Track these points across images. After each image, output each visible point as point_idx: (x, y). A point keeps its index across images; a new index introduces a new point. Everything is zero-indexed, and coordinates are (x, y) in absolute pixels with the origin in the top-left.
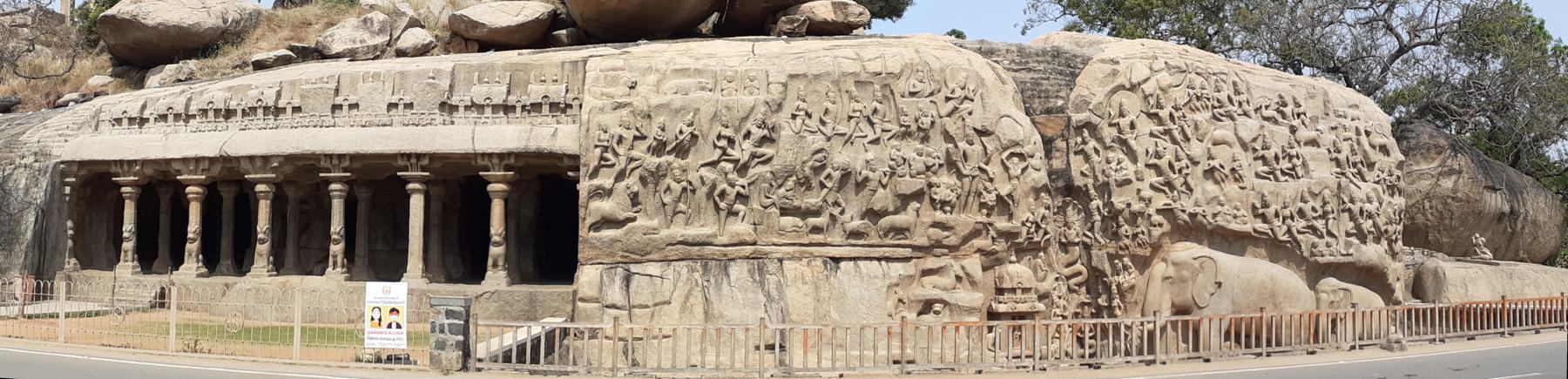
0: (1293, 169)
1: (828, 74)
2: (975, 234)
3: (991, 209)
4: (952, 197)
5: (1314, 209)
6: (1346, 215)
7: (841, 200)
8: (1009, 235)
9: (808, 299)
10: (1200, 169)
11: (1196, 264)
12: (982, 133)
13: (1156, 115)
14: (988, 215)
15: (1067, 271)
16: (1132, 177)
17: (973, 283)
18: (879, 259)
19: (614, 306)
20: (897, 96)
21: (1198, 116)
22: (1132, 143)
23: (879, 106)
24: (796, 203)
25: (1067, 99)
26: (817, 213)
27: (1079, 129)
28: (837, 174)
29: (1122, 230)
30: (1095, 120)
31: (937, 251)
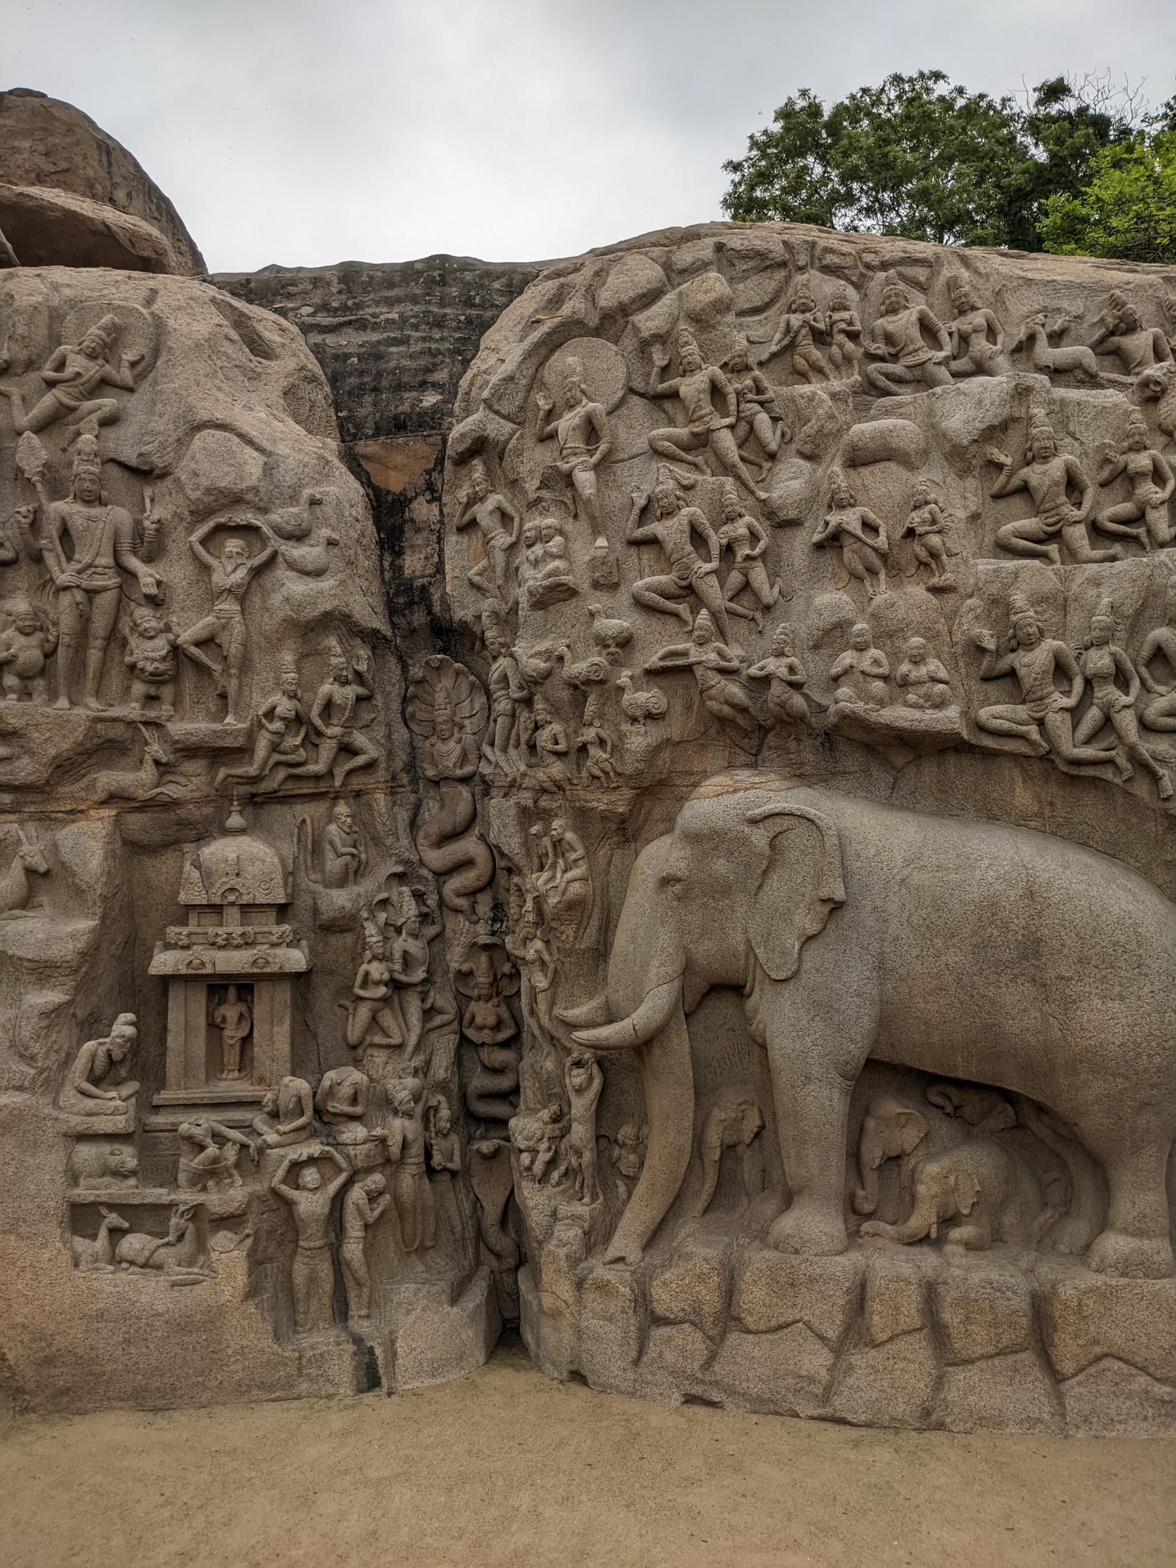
0: (1139, 518)
2: (105, 747)
3: (156, 679)
8: (215, 754)
10: (799, 545)
11: (759, 838)
12: (145, 473)
13: (674, 395)
15: (436, 858)
16: (580, 578)
17: (78, 892)
21: (806, 389)
22: (585, 479)
25: (450, 390)
27: (463, 459)
29: (544, 738)
30: (498, 428)
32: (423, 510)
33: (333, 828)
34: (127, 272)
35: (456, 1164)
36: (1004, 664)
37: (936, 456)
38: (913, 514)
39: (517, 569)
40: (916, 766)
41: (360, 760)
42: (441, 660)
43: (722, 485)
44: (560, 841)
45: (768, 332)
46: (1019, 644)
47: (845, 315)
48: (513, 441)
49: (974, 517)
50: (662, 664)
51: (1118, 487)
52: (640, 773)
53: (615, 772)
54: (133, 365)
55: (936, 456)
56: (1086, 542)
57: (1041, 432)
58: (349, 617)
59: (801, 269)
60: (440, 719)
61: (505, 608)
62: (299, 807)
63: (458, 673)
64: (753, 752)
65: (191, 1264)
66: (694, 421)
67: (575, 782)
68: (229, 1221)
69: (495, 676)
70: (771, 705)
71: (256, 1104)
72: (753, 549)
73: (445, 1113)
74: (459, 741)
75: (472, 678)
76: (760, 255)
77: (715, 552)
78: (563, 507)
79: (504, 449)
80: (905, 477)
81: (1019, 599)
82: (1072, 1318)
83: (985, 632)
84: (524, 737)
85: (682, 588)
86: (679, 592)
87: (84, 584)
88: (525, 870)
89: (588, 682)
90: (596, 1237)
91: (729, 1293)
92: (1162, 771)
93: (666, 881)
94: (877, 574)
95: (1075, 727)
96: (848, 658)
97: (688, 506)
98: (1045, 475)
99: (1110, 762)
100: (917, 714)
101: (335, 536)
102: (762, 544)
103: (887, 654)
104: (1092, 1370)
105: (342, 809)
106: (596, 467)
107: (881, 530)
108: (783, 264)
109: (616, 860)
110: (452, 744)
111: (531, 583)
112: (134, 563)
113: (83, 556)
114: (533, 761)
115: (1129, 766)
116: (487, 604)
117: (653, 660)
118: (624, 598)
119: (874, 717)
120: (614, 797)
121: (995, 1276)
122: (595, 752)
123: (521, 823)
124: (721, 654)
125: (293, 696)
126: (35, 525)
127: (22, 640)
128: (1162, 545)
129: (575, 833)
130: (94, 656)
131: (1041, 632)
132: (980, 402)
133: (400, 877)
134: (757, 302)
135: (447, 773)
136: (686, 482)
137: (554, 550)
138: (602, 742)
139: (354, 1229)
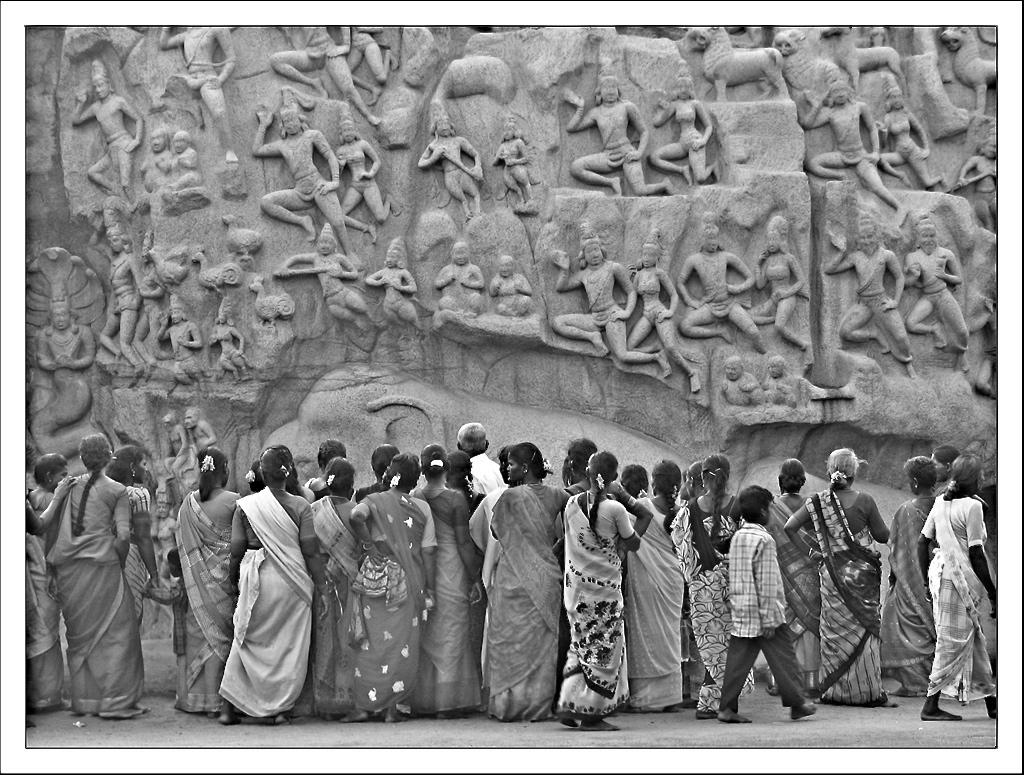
0: (684, 157)
5: (731, 268)
6: (846, 286)
27: (79, 60)
29: (177, 334)
36: (574, 281)
38: (504, 146)
39: (144, 173)
40: (505, 364)
42: (59, 253)
43: (339, 111)
44: (193, 428)
46: (587, 263)
48: (136, 51)
49: (553, 150)
50: (291, 271)
51: (669, 130)
52: (270, 368)
53: (246, 366)
55: (521, 94)
56: (642, 178)
57: (608, 80)
60: (58, 311)
61: (129, 207)
63: (75, 264)
64: (366, 348)
66: (312, 46)
67: (208, 374)
69: (119, 271)
70: (387, 310)
72: (367, 170)
74: (76, 333)
75: (89, 271)
77: (336, 172)
78: (189, 117)
79: (128, 54)
80: (496, 111)
81: (586, 225)
83: (561, 252)
84: (155, 333)
85: (305, 201)
86: (302, 204)
88: (154, 455)
89: (224, 285)
92: (693, 370)
94: (473, 197)
95: (629, 334)
96: (450, 271)
97: (311, 128)
98: (610, 117)
99: (654, 362)
100: (506, 321)
102: (376, 166)
103: (482, 269)
106: (223, 85)
107: (477, 159)
109: (243, 446)
110: (69, 334)
111: (167, 191)
114: (164, 354)
115: (668, 366)
116: (110, 202)
117: (283, 268)
118: (250, 210)
119: (471, 323)
120: (244, 388)
122: (226, 346)
123: (150, 411)
124: (344, 266)
128: (701, 183)
129: (206, 420)
131: (605, 255)
132: (559, 49)
135: (64, 362)
136: (306, 105)
137: (188, 162)
138: (235, 340)
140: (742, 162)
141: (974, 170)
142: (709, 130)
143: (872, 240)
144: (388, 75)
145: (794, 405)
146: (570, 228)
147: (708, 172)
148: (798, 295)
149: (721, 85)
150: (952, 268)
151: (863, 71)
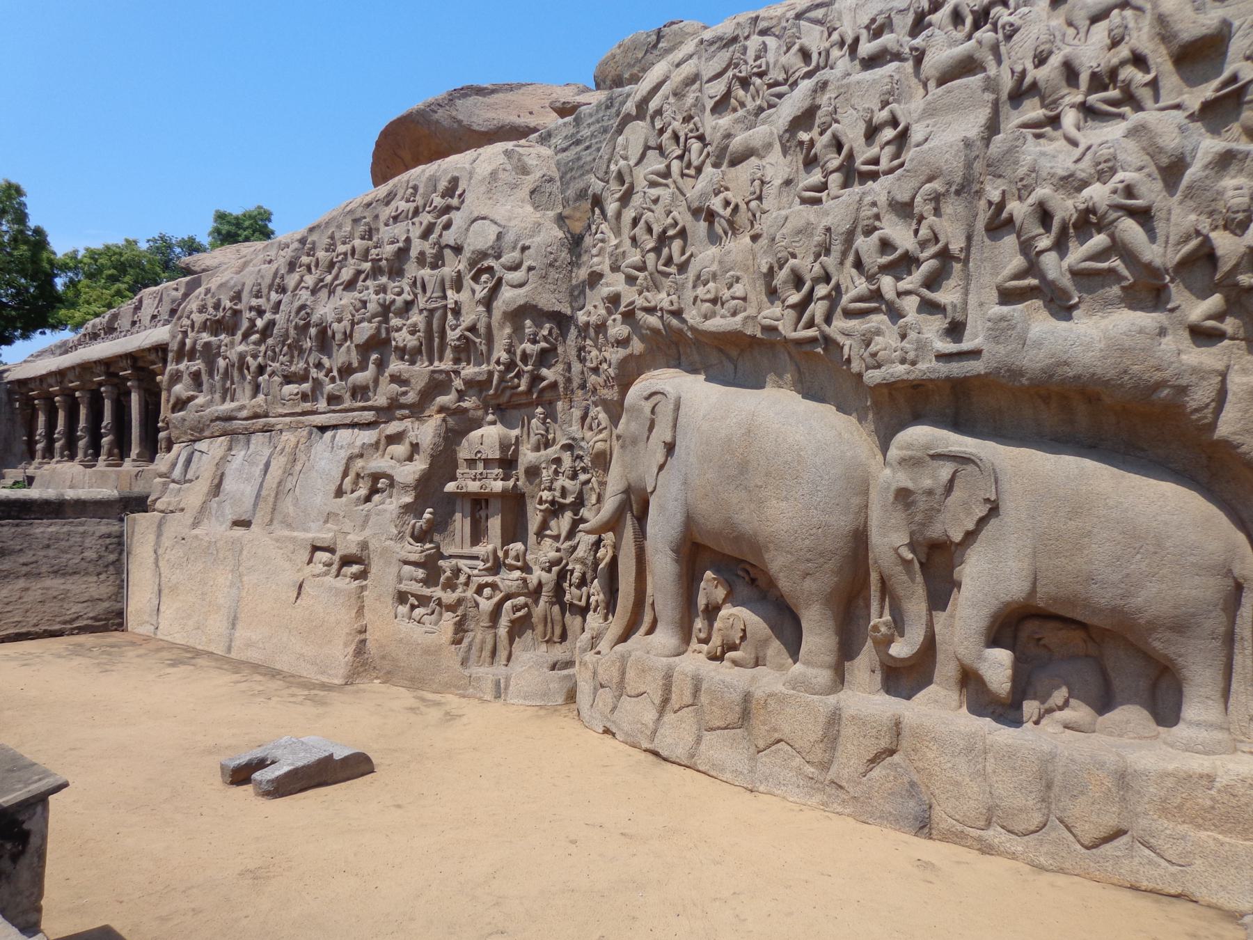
1: (333, 218)
3: (456, 349)
4: (411, 341)
5: (886, 245)
7: (326, 361)
9: (280, 472)
11: (648, 410)
12: (458, 250)
14: (457, 361)
16: (605, 268)
18: (353, 425)
19: (173, 481)
20: (382, 225)
23: (357, 242)
24: (293, 368)
26: (304, 378)
28: (313, 331)
31: (399, 413)
32: (588, 240)
33: (534, 421)
34: (515, 142)
35: (583, 603)
37: (777, 147)
41: (544, 383)
45: (718, 88)
47: (758, 62)
49: (788, 182)
54: (460, 196)
58: (535, 307)
59: (747, 38)
62: (523, 411)
65: (436, 624)
68: (451, 608)
71: (476, 558)
73: (576, 574)
76: (721, 39)
77: (655, 236)
82: (762, 711)
87: (428, 307)
90: (595, 640)
91: (623, 673)
93: (618, 437)
99: (813, 340)
101: (534, 264)
104: (773, 748)
105: (540, 410)
108: (734, 40)
112: (449, 293)
113: (428, 294)
117: (622, 309)
121: (728, 679)
125: (508, 351)
126: (415, 283)
127: (410, 337)
130: (437, 340)
133: (568, 447)
134: (718, 69)
139: (504, 622)
140: (918, 145)
141: (1234, 78)
142: (900, 128)
143: (1024, 182)
144: (703, 162)
145: (913, 363)
146: (773, 239)
147: (896, 162)
148: (945, 255)
149: (932, 84)
150: (1135, 191)
151: (1095, 19)
